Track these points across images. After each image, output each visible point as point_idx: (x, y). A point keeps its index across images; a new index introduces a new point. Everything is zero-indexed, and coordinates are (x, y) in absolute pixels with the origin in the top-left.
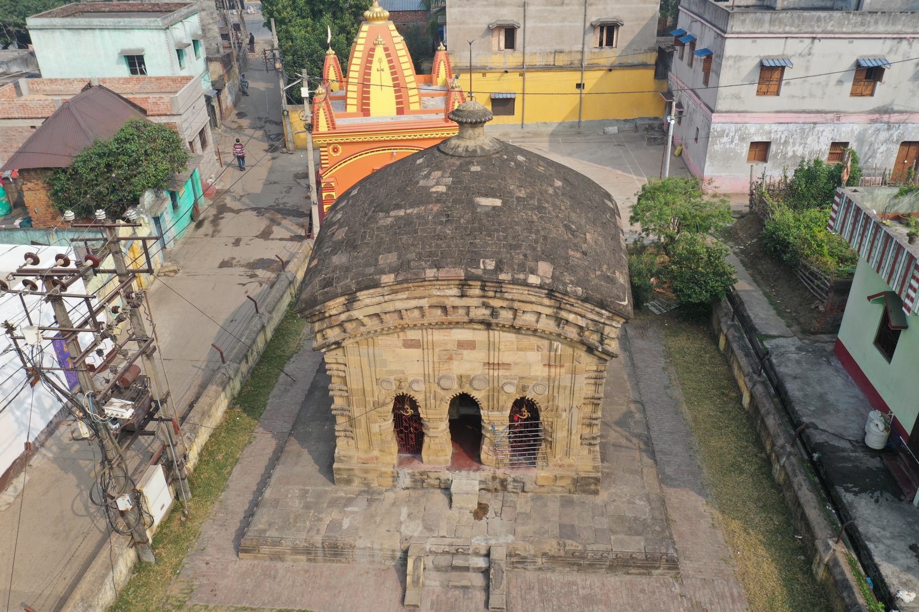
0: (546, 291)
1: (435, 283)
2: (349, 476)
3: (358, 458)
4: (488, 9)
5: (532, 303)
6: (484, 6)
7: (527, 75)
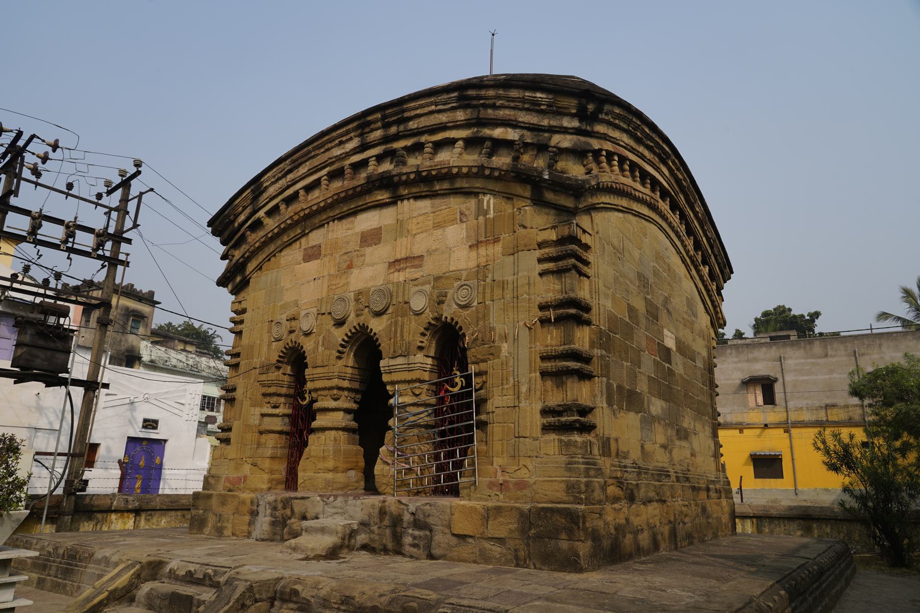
0: (456, 94)
1: (334, 134)
2: (205, 510)
3: (227, 479)
4: (740, 365)
5: (443, 127)
6: (735, 362)
7: (794, 431)
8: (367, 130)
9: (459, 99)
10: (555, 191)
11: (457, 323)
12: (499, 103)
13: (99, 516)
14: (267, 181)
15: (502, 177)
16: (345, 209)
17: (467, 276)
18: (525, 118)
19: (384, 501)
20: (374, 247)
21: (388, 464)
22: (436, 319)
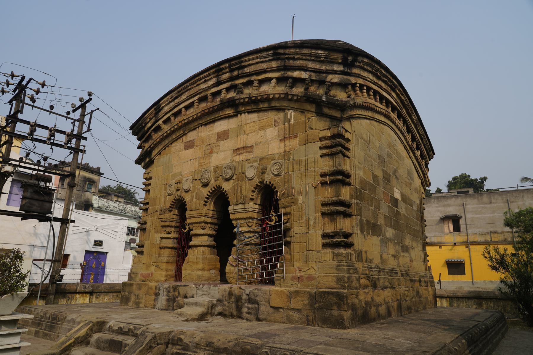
0: (271, 52)
1: (202, 76)
2: (129, 292)
4: (440, 208)
5: (264, 71)
6: (437, 207)
7: (471, 247)
8: (220, 73)
9: (274, 54)
10: (329, 108)
11: (273, 185)
12: (296, 57)
13: (70, 295)
14: (163, 103)
15: (299, 100)
16: (208, 119)
17: (279, 157)
18: (312, 65)
19: (231, 288)
20: (225, 141)
21: (233, 266)
22: (260, 182)
